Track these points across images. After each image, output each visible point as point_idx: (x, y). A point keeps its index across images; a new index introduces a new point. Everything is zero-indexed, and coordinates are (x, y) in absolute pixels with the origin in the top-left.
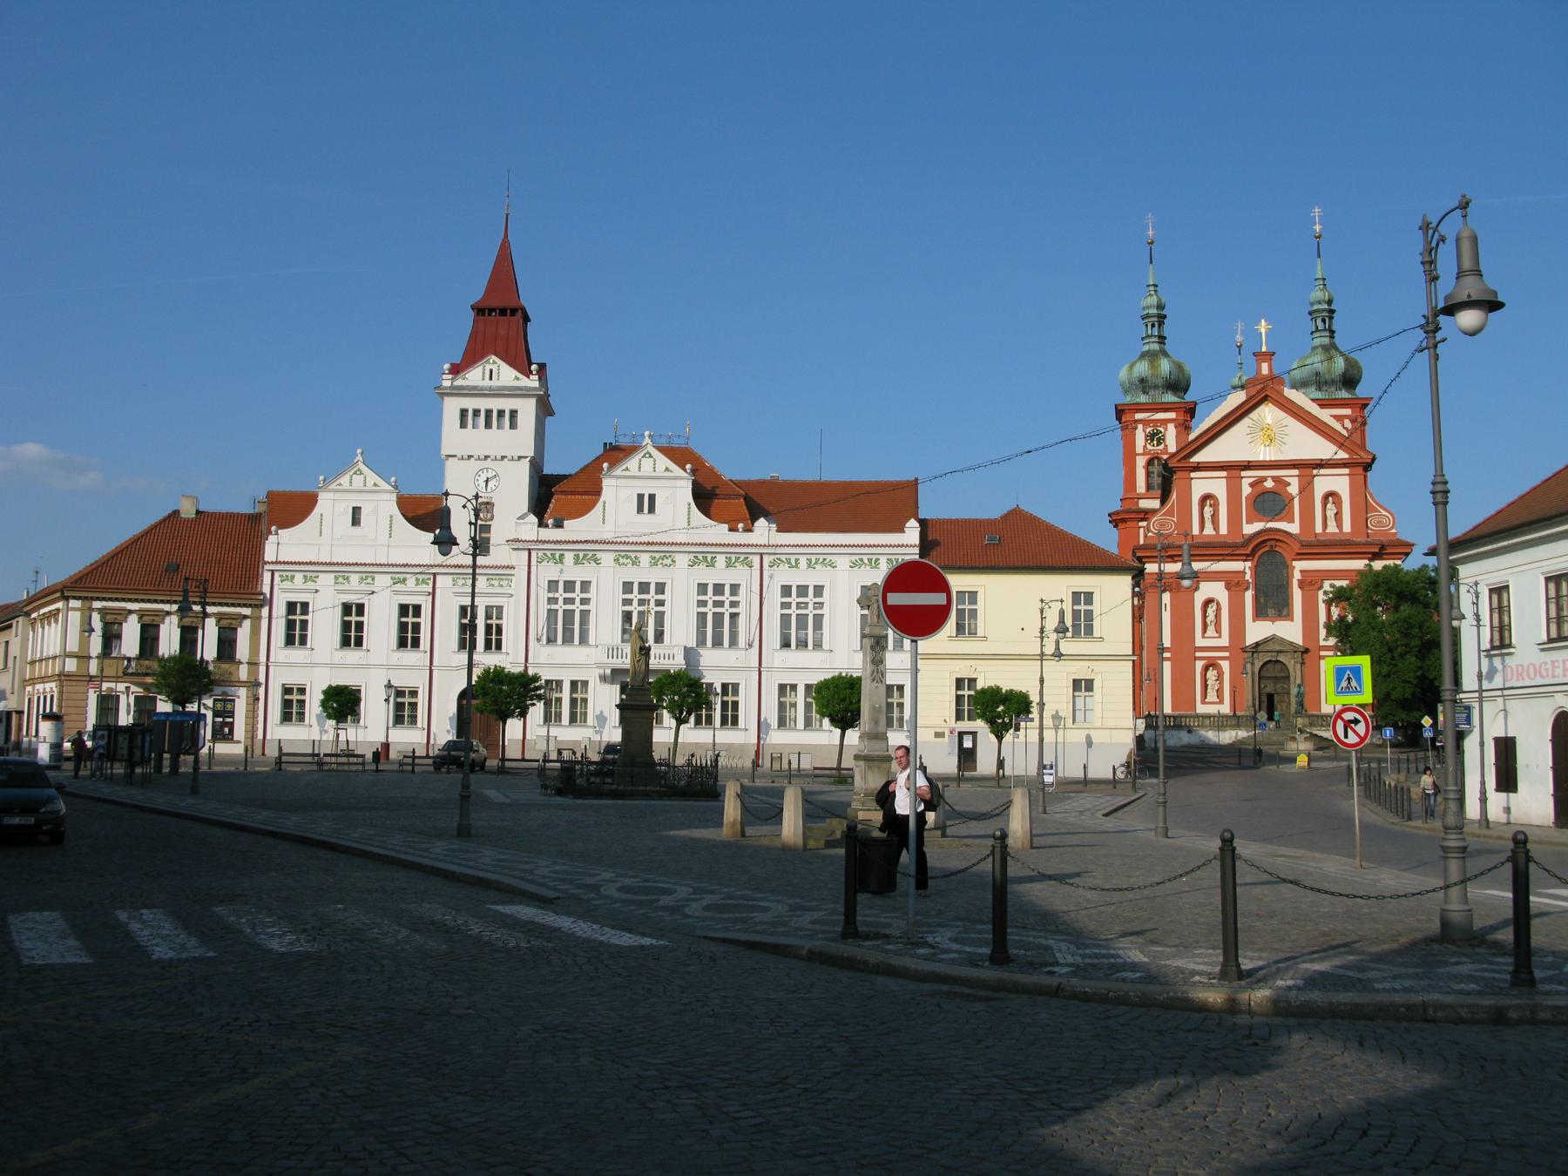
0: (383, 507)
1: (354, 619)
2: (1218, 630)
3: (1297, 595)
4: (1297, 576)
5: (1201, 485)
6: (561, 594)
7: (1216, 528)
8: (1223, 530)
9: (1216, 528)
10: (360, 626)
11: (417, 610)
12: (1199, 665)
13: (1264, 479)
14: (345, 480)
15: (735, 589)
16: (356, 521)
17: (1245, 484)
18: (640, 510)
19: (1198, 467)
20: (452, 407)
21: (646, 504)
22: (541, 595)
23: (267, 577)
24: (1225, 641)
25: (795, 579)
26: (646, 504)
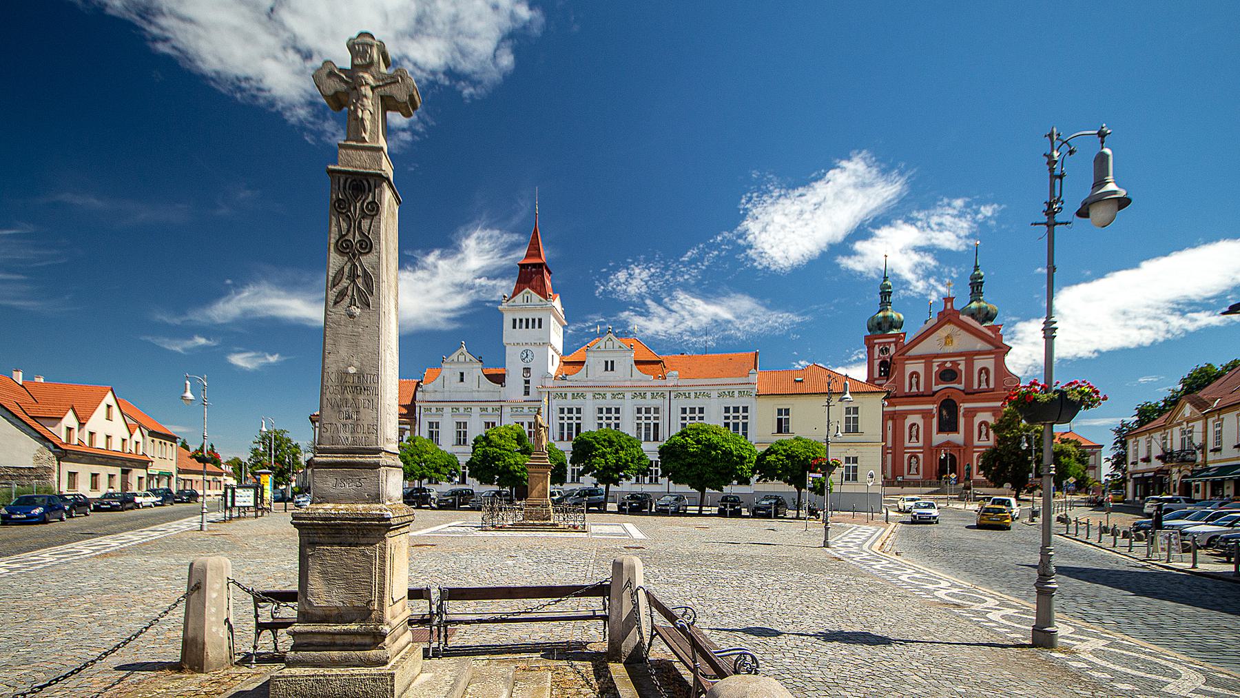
0: (475, 371)
3: (962, 421)
4: (962, 411)
5: (910, 367)
6: (566, 415)
8: (922, 390)
14: (454, 357)
15: (657, 410)
16: (462, 380)
19: (910, 358)
21: (610, 366)
22: (555, 414)
25: (688, 404)
26: (610, 366)
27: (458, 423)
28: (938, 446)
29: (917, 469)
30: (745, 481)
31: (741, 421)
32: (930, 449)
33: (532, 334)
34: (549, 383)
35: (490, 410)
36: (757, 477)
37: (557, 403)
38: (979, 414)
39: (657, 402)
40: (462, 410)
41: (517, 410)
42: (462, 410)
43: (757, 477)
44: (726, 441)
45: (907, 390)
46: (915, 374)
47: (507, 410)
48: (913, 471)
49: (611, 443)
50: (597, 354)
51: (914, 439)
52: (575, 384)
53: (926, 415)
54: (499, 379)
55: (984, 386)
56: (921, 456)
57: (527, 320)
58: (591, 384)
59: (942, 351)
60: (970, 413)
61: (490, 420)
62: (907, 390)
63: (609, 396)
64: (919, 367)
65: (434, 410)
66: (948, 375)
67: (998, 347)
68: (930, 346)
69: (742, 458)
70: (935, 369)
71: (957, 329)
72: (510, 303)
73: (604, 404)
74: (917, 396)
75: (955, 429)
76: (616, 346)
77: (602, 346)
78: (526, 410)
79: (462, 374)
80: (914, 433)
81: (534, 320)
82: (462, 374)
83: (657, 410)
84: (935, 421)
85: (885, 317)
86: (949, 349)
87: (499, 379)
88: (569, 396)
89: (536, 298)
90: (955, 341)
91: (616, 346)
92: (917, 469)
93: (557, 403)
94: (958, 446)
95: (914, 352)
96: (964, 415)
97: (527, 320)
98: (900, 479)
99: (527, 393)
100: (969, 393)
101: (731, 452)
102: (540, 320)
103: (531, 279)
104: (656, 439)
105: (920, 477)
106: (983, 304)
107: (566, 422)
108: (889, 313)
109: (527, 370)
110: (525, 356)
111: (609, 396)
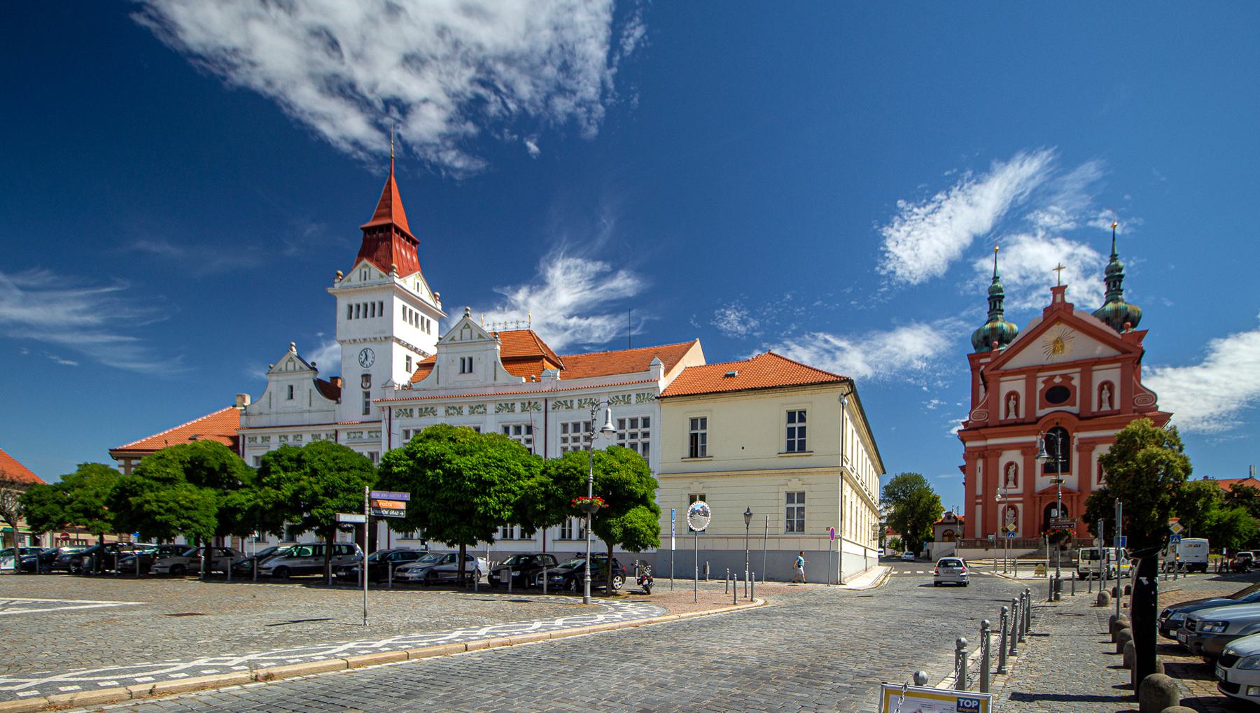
2: (1016, 483)
3: (1075, 457)
5: (1006, 386)
7: (1017, 414)
8: (1022, 415)
9: (1017, 414)
13: (1055, 376)
17: (1040, 380)
24: (1020, 490)
28: (1043, 492)
32: (1031, 495)
45: (1002, 417)
46: (1013, 395)
51: (1011, 484)
53: (1029, 451)
55: (1106, 407)
56: (1020, 506)
59: (1049, 362)
62: (1002, 417)
64: (1017, 385)
66: (1058, 394)
67: (1125, 352)
70: (1040, 386)
71: (1068, 329)
74: (1015, 424)
75: (1066, 469)
80: (1011, 475)
85: (993, 329)
86: (1058, 358)
90: (1067, 346)
95: (1014, 363)
96: (1079, 449)
98: (991, 537)
105: (1019, 535)
108: (999, 324)
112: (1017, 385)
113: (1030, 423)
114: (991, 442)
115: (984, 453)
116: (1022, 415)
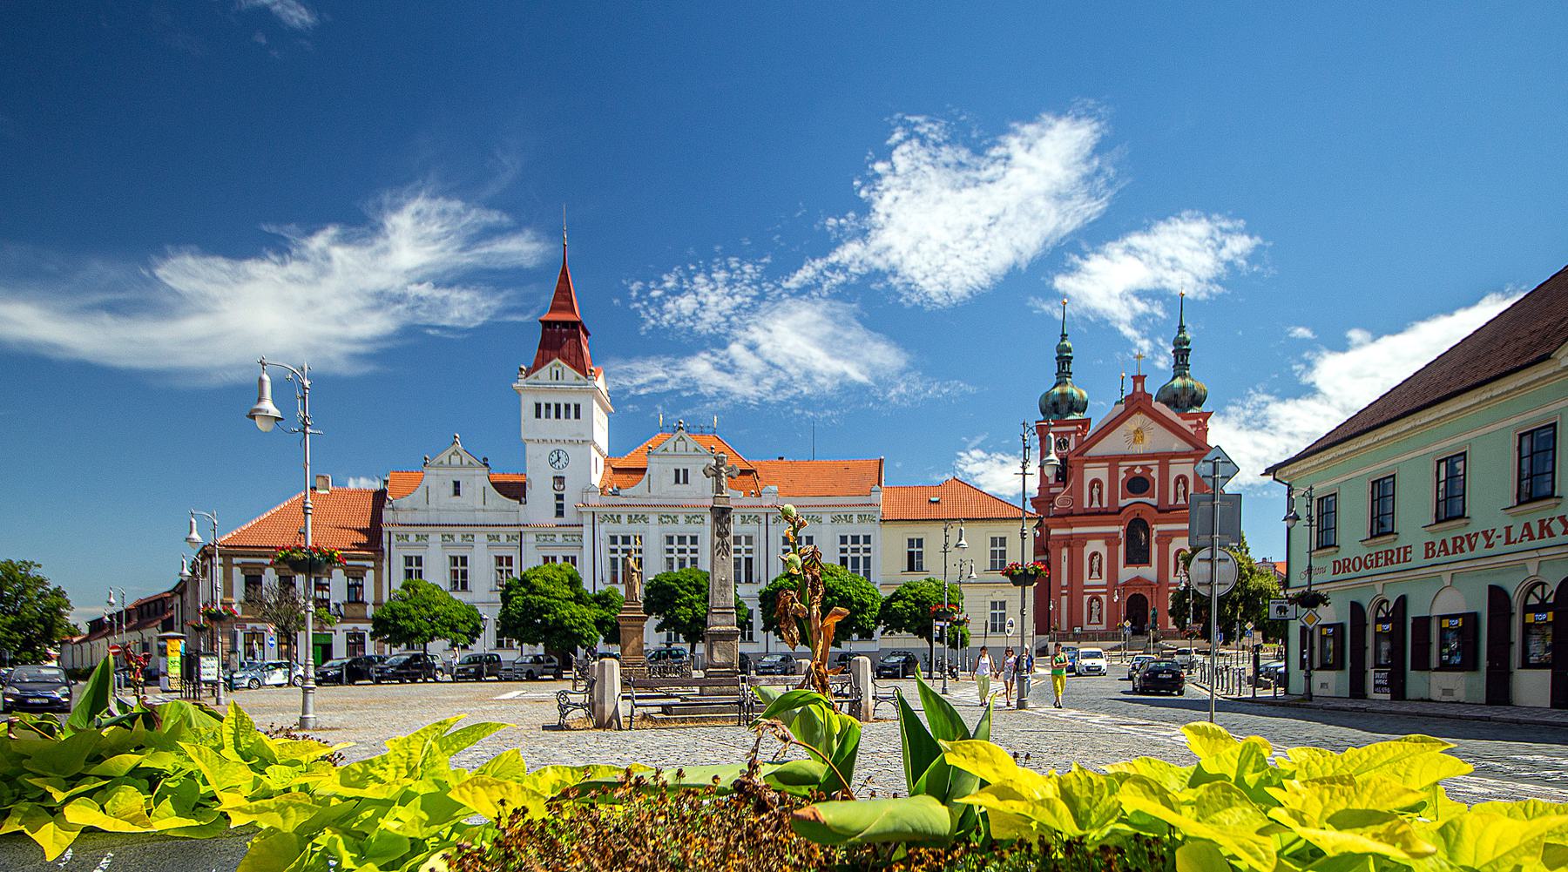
0: (477, 482)
1: (460, 568)
8: (1105, 505)
10: (464, 574)
11: (509, 559)
12: (1086, 598)
15: (749, 540)
16: (457, 493)
17: (1122, 470)
18: (677, 481)
20: (528, 404)
21: (681, 477)
22: (604, 546)
23: (385, 537)
26: (681, 477)
27: (454, 560)
29: (1100, 617)
30: (867, 635)
31: (861, 555)
33: (567, 426)
34: (594, 500)
35: (503, 539)
36: (881, 628)
37: (604, 530)
38: (1175, 540)
39: (751, 528)
40: (458, 538)
41: (544, 536)
42: (458, 538)
43: (881, 628)
44: (845, 584)
45: (1086, 505)
47: (530, 539)
48: (1095, 619)
49: (699, 589)
50: (662, 459)
51: (1095, 574)
52: (633, 501)
53: (1111, 540)
54: (515, 490)
56: (1104, 598)
57: (558, 406)
58: (655, 502)
59: (1130, 452)
60: (1166, 538)
61: (504, 553)
62: (1086, 505)
63: (682, 519)
65: (412, 538)
66: (1138, 485)
68: (1113, 444)
69: (863, 605)
70: (1122, 476)
71: (1149, 420)
72: (531, 378)
73: (676, 530)
74: (1099, 513)
75: (1146, 561)
76: (691, 447)
77: (671, 448)
78: (559, 538)
79: (457, 484)
80: (1096, 566)
81: (567, 407)
82: (457, 484)
83: (749, 540)
84: (1121, 549)
86: (1139, 449)
87: (515, 490)
88: (624, 519)
89: (570, 373)
90: (1147, 438)
91: (691, 447)
92: (1100, 617)
93: (604, 530)
94: (1150, 583)
95: (1096, 450)
97: (558, 406)
98: (1077, 630)
99: (560, 513)
100: (1164, 511)
101: (850, 599)
102: (577, 407)
103: (561, 345)
104: (749, 579)
105: (1103, 627)
106: (1189, 381)
107: (620, 556)
109: (560, 480)
110: (556, 458)
111: (682, 519)
112: (1100, 472)
113: (1112, 513)
114: (1075, 530)
115: (1069, 541)
116: (1105, 505)
